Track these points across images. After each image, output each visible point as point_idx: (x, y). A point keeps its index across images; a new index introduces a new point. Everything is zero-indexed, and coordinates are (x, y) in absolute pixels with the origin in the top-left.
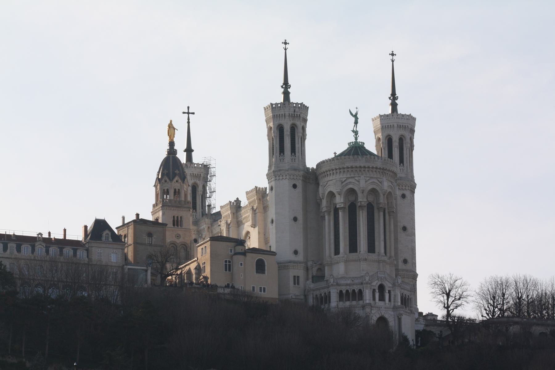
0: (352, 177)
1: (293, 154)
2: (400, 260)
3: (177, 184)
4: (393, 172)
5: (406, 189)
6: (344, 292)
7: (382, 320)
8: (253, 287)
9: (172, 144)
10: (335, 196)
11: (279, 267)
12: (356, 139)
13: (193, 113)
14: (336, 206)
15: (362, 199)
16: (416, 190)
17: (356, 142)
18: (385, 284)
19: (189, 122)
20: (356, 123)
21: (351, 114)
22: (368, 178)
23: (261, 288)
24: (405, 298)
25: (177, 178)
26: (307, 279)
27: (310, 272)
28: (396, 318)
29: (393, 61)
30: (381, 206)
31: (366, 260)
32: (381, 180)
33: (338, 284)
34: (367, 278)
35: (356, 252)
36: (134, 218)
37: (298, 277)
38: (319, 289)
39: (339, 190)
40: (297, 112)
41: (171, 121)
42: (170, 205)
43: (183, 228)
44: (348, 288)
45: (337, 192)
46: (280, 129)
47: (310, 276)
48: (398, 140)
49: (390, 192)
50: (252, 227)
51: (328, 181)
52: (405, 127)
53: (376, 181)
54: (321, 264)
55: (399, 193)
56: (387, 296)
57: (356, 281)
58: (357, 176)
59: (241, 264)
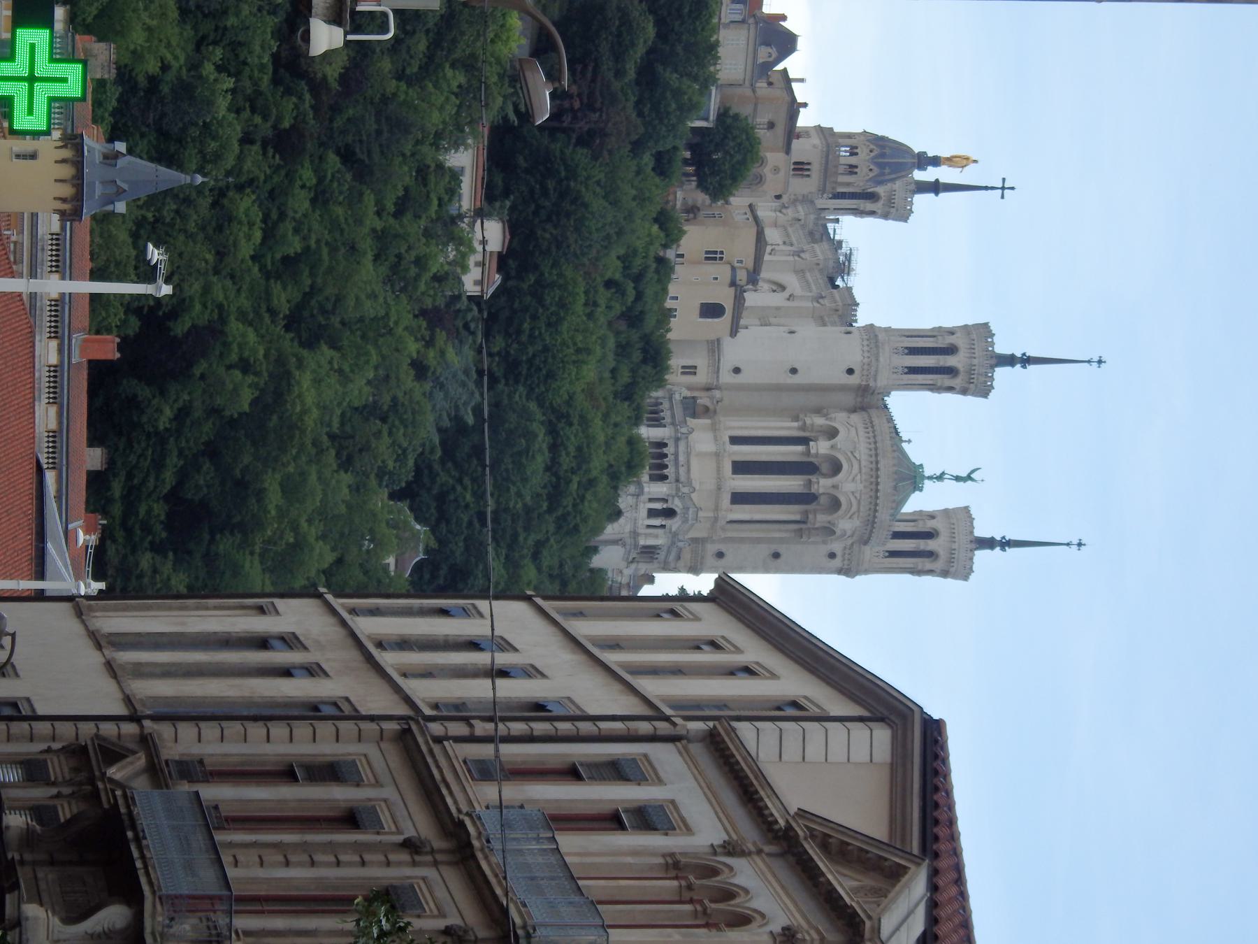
0: (860, 469)
1: (906, 370)
3: (865, 170)
4: (869, 539)
5: (844, 560)
6: (665, 450)
7: (618, 514)
8: (676, 298)
9: (936, 161)
10: (830, 440)
11: (712, 342)
12: (930, 478)
13: (1003, 197)
14: (812, 440)
15: (822, 485)
16: (842, 578)
17: (923, 478)
19: (986, 188)
20: (958, 479)
21: (973, 471)
22: (858, 495)
24: (653, 553)
25: (876, 171)
26: (690, 388)
27: (703, 394)
28: (618, 537)
29: (1068, 544)
30: (811, 516)
31: (719, 488)
33: (677, 440)
34: (685, 490)
36: (799, 100)
37: (695, 373)
38: (672, 408)
39: (839, 447)
40: (978, 379)
41: (975, 161)
44: (671, 457)
45: (837, 444)
46: (951, 350)
47: (696, 394)
48: (929, 548)
49: (833, 533)
50: (790, 296)
51: (856, 429)
52: (951, 561)
53: (854, 508)
54: (715, 412)
55: (837, 547)
56: (657, 522)
57: (682, 471)
58: (863, 479)
59: (716, 279)
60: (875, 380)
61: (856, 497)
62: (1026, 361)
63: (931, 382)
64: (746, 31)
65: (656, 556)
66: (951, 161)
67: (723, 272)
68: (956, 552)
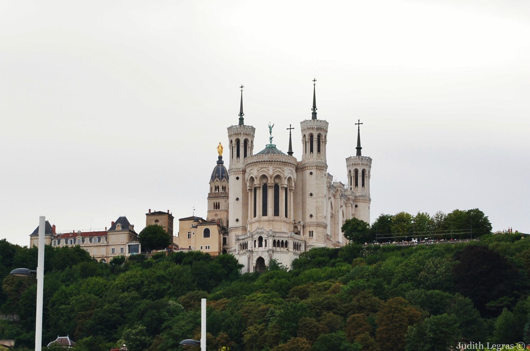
2: (308, 216)
3: (217, 183)
8: (202, 247)
9: (220, 158)
12: (271, 143)
17: (271, 145)
18: (262, 236)
19: (290, 135)
23: (206, 247)
32: (269, 168)
33: (238, 240)
35: (267, 215)
36: (148, 212)
40: (239, 131)
42: (212, 196)
43: (220, 209)
56: (264, 243)
59: (194, 233)
60: (240, 169)
61: (260, 170)
62: (241, 113)
63: (250, 149)
64: (110, 235)
65: (285, 241)
66: (220, 152)
67: (193, 230)
68: (308, 127)
